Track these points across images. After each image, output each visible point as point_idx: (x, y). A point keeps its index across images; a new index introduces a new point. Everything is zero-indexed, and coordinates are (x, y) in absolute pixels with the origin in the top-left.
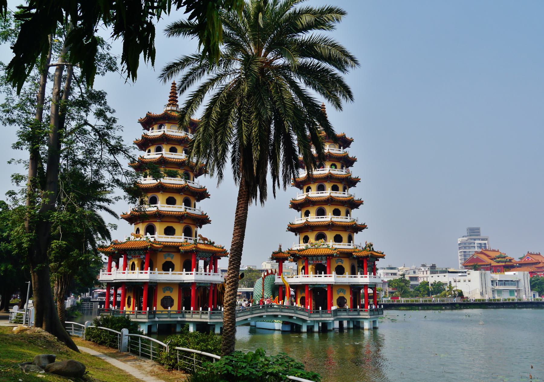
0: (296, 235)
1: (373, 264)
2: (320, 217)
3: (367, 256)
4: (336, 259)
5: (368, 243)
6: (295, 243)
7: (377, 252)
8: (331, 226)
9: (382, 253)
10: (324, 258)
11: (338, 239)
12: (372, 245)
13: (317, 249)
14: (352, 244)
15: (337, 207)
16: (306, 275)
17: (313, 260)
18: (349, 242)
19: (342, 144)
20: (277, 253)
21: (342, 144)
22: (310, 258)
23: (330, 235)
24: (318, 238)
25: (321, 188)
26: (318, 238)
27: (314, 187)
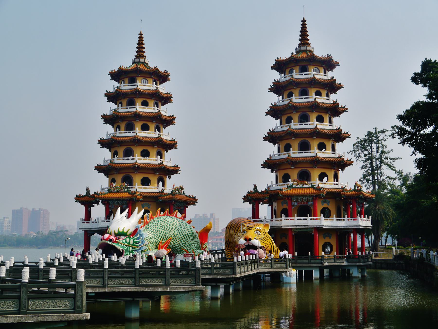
1: (182, 208)
3: (172, 200)
4: (142, 203)
8: (137, 168)
9: (195, 197)
10: (124, 202)
11: (145, 182)
16: (108, 220)
19: (156, 78)
20: (83, 197)
21: (156, 78)
22: (110, 202)
23: (137, 179)
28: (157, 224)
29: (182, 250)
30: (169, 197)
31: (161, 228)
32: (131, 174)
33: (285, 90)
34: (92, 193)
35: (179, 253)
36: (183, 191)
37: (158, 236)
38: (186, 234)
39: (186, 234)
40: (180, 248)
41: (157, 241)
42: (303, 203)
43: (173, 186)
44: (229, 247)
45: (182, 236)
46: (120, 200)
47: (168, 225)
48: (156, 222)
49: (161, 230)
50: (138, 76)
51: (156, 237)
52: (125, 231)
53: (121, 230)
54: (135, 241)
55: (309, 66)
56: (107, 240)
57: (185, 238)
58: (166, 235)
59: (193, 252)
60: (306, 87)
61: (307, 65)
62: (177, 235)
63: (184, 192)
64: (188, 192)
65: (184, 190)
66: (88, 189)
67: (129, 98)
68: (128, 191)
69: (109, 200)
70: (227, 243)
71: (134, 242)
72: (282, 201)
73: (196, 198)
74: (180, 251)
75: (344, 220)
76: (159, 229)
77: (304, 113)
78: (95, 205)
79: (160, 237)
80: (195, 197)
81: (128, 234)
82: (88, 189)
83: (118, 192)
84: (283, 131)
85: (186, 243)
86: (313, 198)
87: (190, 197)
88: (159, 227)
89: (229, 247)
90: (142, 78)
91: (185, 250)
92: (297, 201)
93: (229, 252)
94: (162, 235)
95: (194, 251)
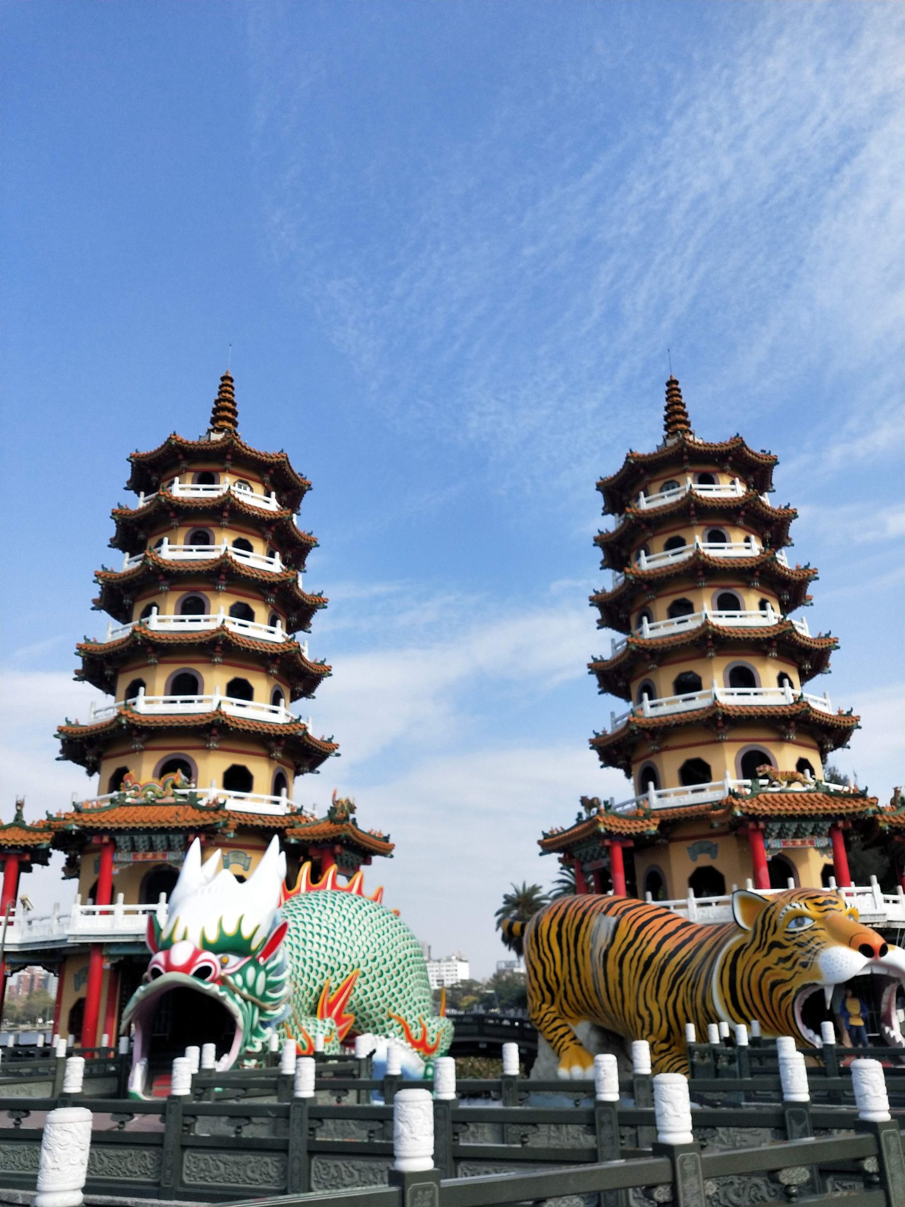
0: (90, 773)
2: (178, 698)
3: (336, 841)
5: (342, 796)
6: (73, 789)
7: (369, 834)
8: (215, 731)
9: (386, 839)
11: (238, 780)
12: (352, 809)
13: (151, 804)
14: (283, 799)
15: (242, 674)
17: (134, 849)
18: (277, 792)
19: (270, 488)
22: (121, 840)
23: (211, 767)
24: (167, 768)
25: (194, 606)
26: (167, 768)
27: (171, 602)
28: (307, 919)
29: (390, 1019)
30: (327, 827)
31: (324, 932)
32: (191, 753)
33: (655, 535)
34: (32, 817)
35: (376, 1032)
36: (351, 816)
37: (315, 965)
38: (401, 956)
39: (401, 956)
40: (383, 1011)
41: (310, 985)
42: (799, 842)
43: (334, 795)
44: (552, 1003)
45: (389, 964)
46: (162, 831)
47: (346, 923)
48: (304, 912)
49: (323, 941)
50: (224, 471)
51: (307, 969)
52: (246, 933)
53: (230, 929)
54: (271, 978)
55: (718, 475)
56: (186, 969)
57: (398, 973)
58: (340, 958)
59: (422, 1026)
60: (721, 526)
61: (715, 472)
62: (374, 960)
63: (354, 819)
64: (367, 821)
65: (357, 815)
66: (20, 805)
67: (194, 526)
68: (192, 800)
69: (120, 831)
70: (549, 988)
71: (270, 986)
72: (690, 843)
73: (391, 841)
74: (382, 1022)
75: (895, 902)
76: (317, 937)
77: (729, 591)
78: (36, 867)
79: (322, 969)
80: (386, 839)
81: (254, 945)
82: (20, 805)
83: (151, 804)
84: (673, 635)
85: (401, 991)
86: (834, 827)
87: (374, 836)
88: (317, 929)
89: (552, 1003)
90: (236, 478)
91: (398, 1018)
92: (779, 836)
93: (558, 1023)
94: (326, 960)
95: (425, 1023)
